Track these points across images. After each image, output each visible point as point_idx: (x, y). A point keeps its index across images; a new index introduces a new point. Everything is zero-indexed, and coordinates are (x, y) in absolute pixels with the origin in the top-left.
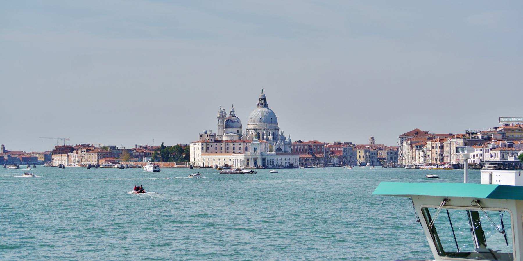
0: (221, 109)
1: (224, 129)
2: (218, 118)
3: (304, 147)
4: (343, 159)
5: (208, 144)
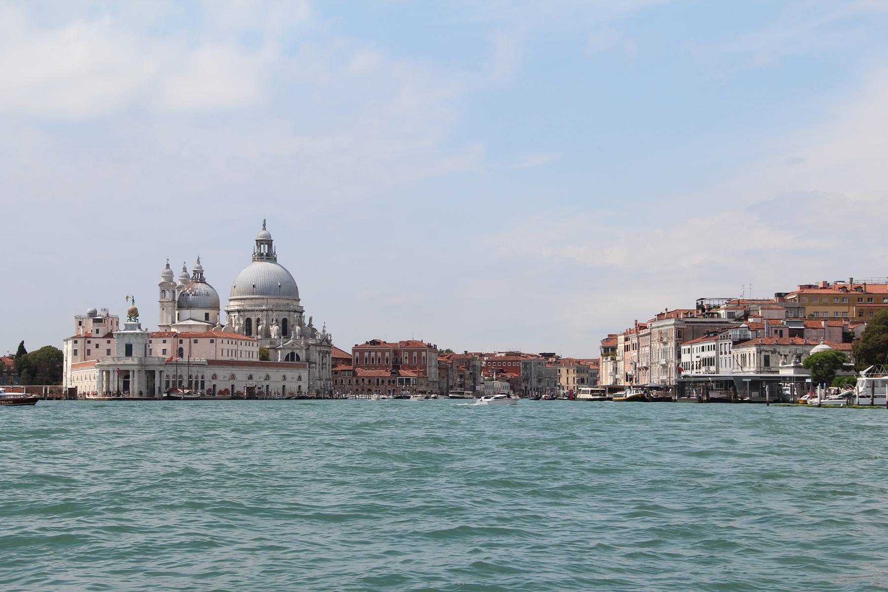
0: (168, 265)
3: (383, 354)
4: (523, 385)
5: (89, 342)
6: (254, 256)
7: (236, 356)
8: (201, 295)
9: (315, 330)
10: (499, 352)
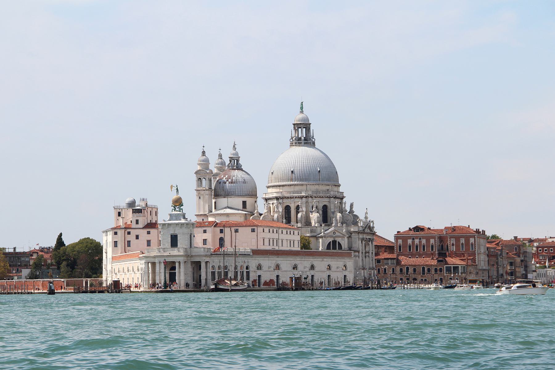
0: (204, 153)
1: (214, 201)
2: (196, 173)
3: (428, 241)
5: (129, 233)
6: (291, 140)
7: (277, 245)
8: (238, 182)
9: (356, 217)
10: (551, 238)
